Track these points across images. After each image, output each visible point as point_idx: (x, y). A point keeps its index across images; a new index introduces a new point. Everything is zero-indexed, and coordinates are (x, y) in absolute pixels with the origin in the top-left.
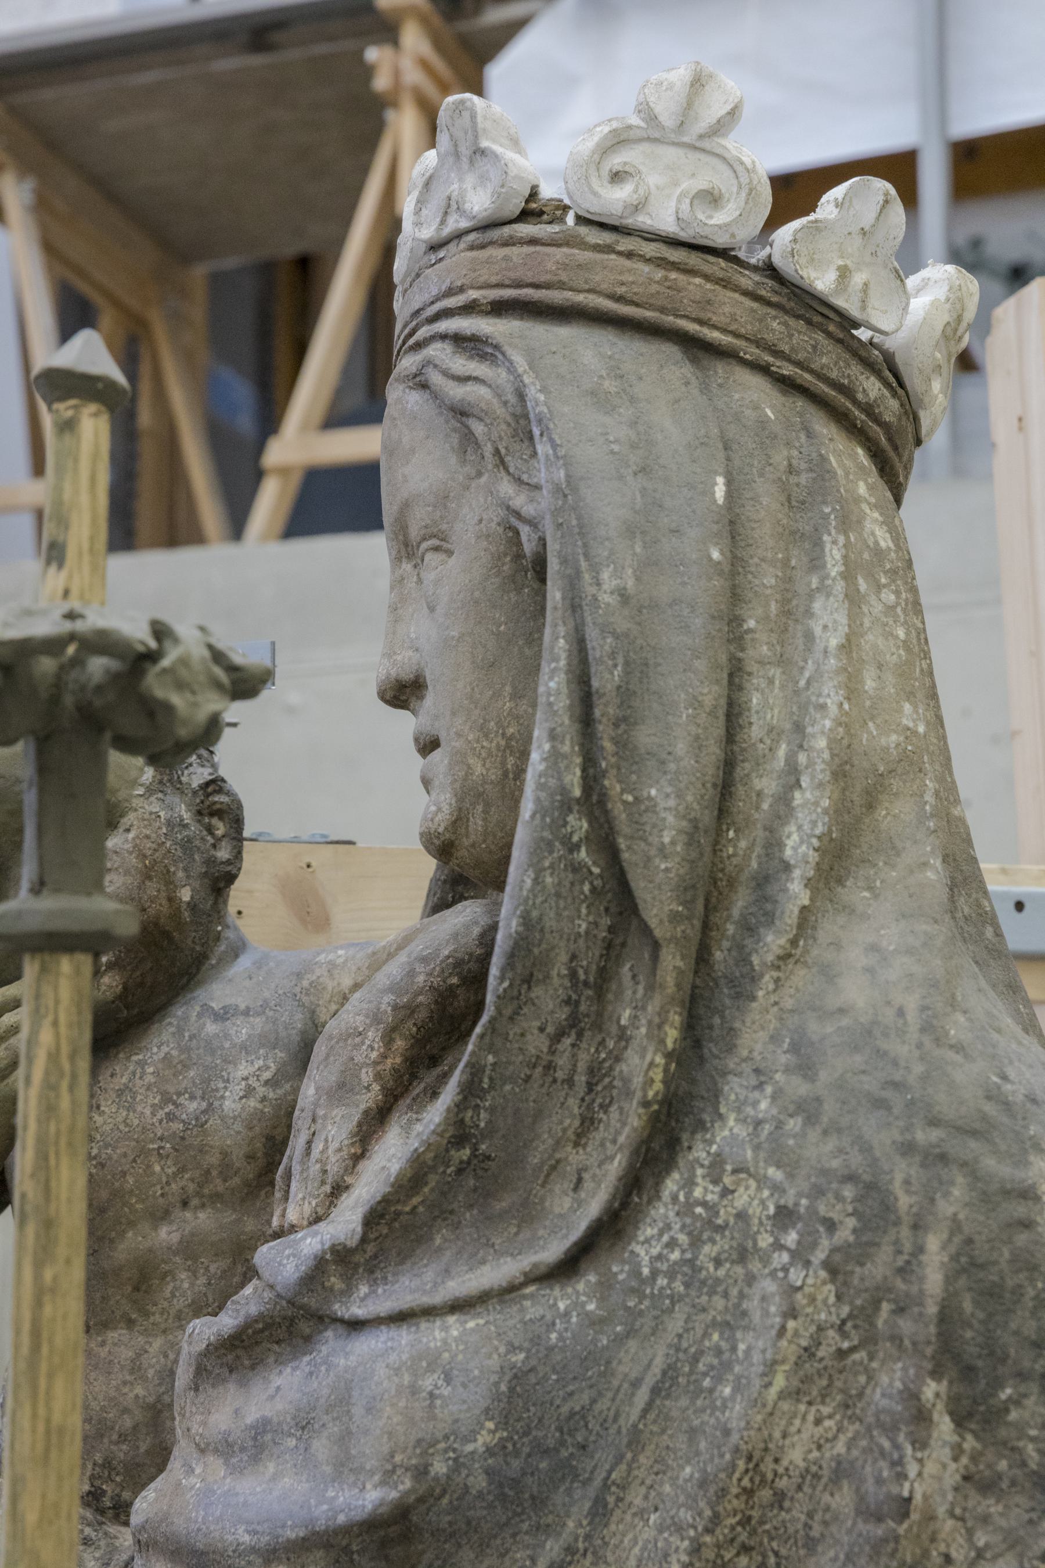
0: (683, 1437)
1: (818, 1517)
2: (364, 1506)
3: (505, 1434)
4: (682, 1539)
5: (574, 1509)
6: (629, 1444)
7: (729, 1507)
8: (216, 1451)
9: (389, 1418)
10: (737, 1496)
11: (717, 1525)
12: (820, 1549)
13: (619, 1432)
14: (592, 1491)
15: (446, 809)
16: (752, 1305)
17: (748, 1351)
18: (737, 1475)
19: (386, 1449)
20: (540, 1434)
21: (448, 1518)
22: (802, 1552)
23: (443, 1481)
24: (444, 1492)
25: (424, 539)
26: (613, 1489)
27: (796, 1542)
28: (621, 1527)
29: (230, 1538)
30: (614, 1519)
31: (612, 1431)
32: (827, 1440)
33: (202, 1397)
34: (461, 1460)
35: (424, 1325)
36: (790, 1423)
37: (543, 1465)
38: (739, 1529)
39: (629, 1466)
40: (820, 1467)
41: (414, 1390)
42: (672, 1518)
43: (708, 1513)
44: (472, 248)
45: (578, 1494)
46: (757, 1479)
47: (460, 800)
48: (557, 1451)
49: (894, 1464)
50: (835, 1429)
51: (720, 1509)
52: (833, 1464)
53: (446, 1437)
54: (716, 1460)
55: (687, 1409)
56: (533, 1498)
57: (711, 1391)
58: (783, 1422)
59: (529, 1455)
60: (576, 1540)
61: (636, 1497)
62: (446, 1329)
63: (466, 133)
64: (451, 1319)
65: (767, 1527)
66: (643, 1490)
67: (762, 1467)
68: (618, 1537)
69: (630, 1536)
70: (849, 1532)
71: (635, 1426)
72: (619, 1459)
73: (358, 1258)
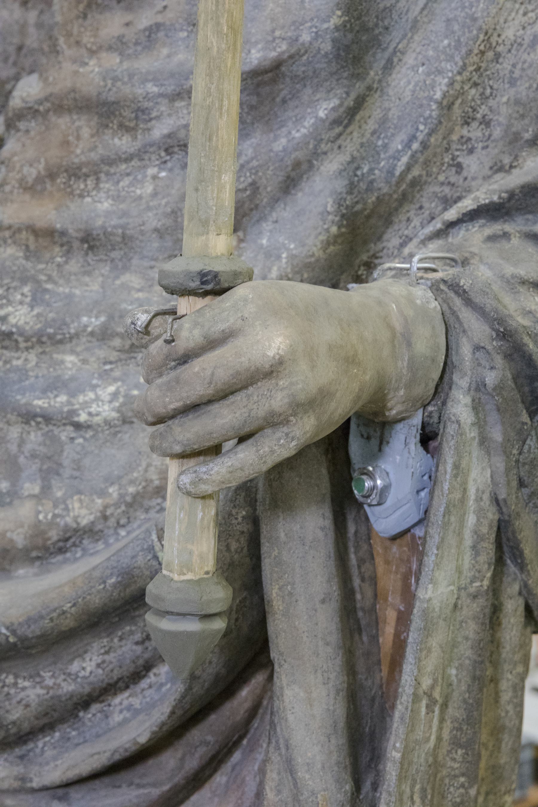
1: (519, 66)
2: (251, 62)
3: (347, 18)
4: (444, 78)
5: (375, 65)
6: (411, 29)
7: (472, 61)
8: (110, 48)
9: (272, 10)
10: (476, 55)
11: (464, 70)
12: (518, 83)
13: (407, 21)
14: (387, 55)
18: (478, 43)
20: (367, 19)
21: (303, 69)
22: (507, 86)
23: (307, 45)
24: (306, 52)
26: (398, 54)
27: (503, 82)
28: (399, 76)
29: (140, 91)
30: (395, 71)
31: (404, 20)
32: (529, 24)
33: (88, 22)
34: (320, 33)
36: (509, 15)
37: (364, 38)
38: (474, 73)
39: (409, 41)
40: (523, 39)
42: (436, 68)
43: (461, 63)
45: (379, 56)
46: (488, 45)
48: (373, 29)
50: (534, 18)
51: (467, 61)
52: (531, 38)
53: (312, 19)
54: (467, 35)
55: (445, 8)
56: (354, 57)
58: (506, 14)
59: (358, 32)
60: (373, 82)
61: (410, 59)
65: (488, 73)
66: (414, 55)
67: (492, 40)
68: (397, 81)
69: (405, 80)
71: (416, 18)
72: (405, 36)
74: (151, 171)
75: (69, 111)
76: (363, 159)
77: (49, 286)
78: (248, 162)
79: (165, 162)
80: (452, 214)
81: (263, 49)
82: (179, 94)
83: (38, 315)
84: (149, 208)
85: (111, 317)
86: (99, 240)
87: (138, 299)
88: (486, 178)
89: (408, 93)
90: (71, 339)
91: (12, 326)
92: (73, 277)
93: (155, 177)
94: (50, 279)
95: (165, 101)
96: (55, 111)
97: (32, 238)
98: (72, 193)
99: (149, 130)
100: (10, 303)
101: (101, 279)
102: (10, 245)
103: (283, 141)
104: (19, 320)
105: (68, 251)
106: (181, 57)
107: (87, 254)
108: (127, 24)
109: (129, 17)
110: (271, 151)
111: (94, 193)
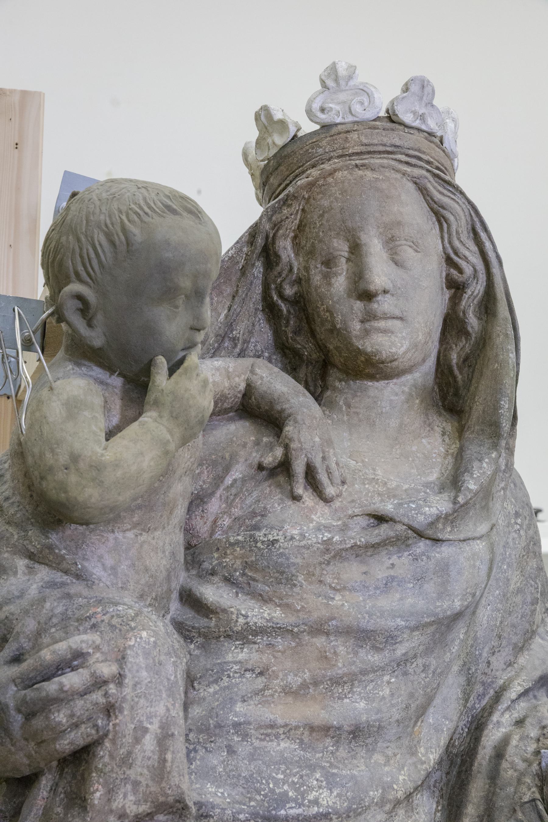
0: (495, 582)
8: (353, 589)
15: (405, 347)
16: (510, 540)
17: (510, 554)
19: (465, 587)
25: (406, 240)
29: (392, 624)
33: (331, 567)
35: (471, 542)
41: (474, 566)
44: (426, 138)
47: (410, 345)
49: (535, 589)
57: (501, 567)
62: (478, 545)
63: (428, 94)
64: (478, 542)
70: (521, 609)
73: (450, 518)
74: (386, 678)
75: (327, 634)
76: (470, 663)
77: (335, 771)
78: (435, 670)
79: (394, 672)
80: (514, 696)
81: (461, 600)
82: (417, 628)
83: (339, 795)
84: (393, 706)
85: (384, 789)
86: (363, 731)
87: (388, 772)
88: (504, 670)
89: (485, 622)
90: (366, 810)
91: (327, 807)
92: (346, 761)
93: (389, 683)
94: (332, 765)
95: (408, 631)
96: (308, 633)
97: (307, 733)
98: (332, 696)
99: (394, 650)
100: (311, 789)
101: (363, 760)
102: (282, 740)
103: (448, 654)
104: (327, 801)
105: (337, 742)
106: (410, 601)
107: (351, 742)
108: (365, 573)
109: (364, 569)
110: (444, 661)
111: (350, 695)
